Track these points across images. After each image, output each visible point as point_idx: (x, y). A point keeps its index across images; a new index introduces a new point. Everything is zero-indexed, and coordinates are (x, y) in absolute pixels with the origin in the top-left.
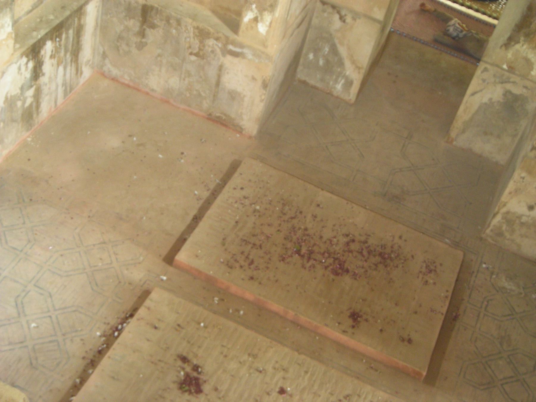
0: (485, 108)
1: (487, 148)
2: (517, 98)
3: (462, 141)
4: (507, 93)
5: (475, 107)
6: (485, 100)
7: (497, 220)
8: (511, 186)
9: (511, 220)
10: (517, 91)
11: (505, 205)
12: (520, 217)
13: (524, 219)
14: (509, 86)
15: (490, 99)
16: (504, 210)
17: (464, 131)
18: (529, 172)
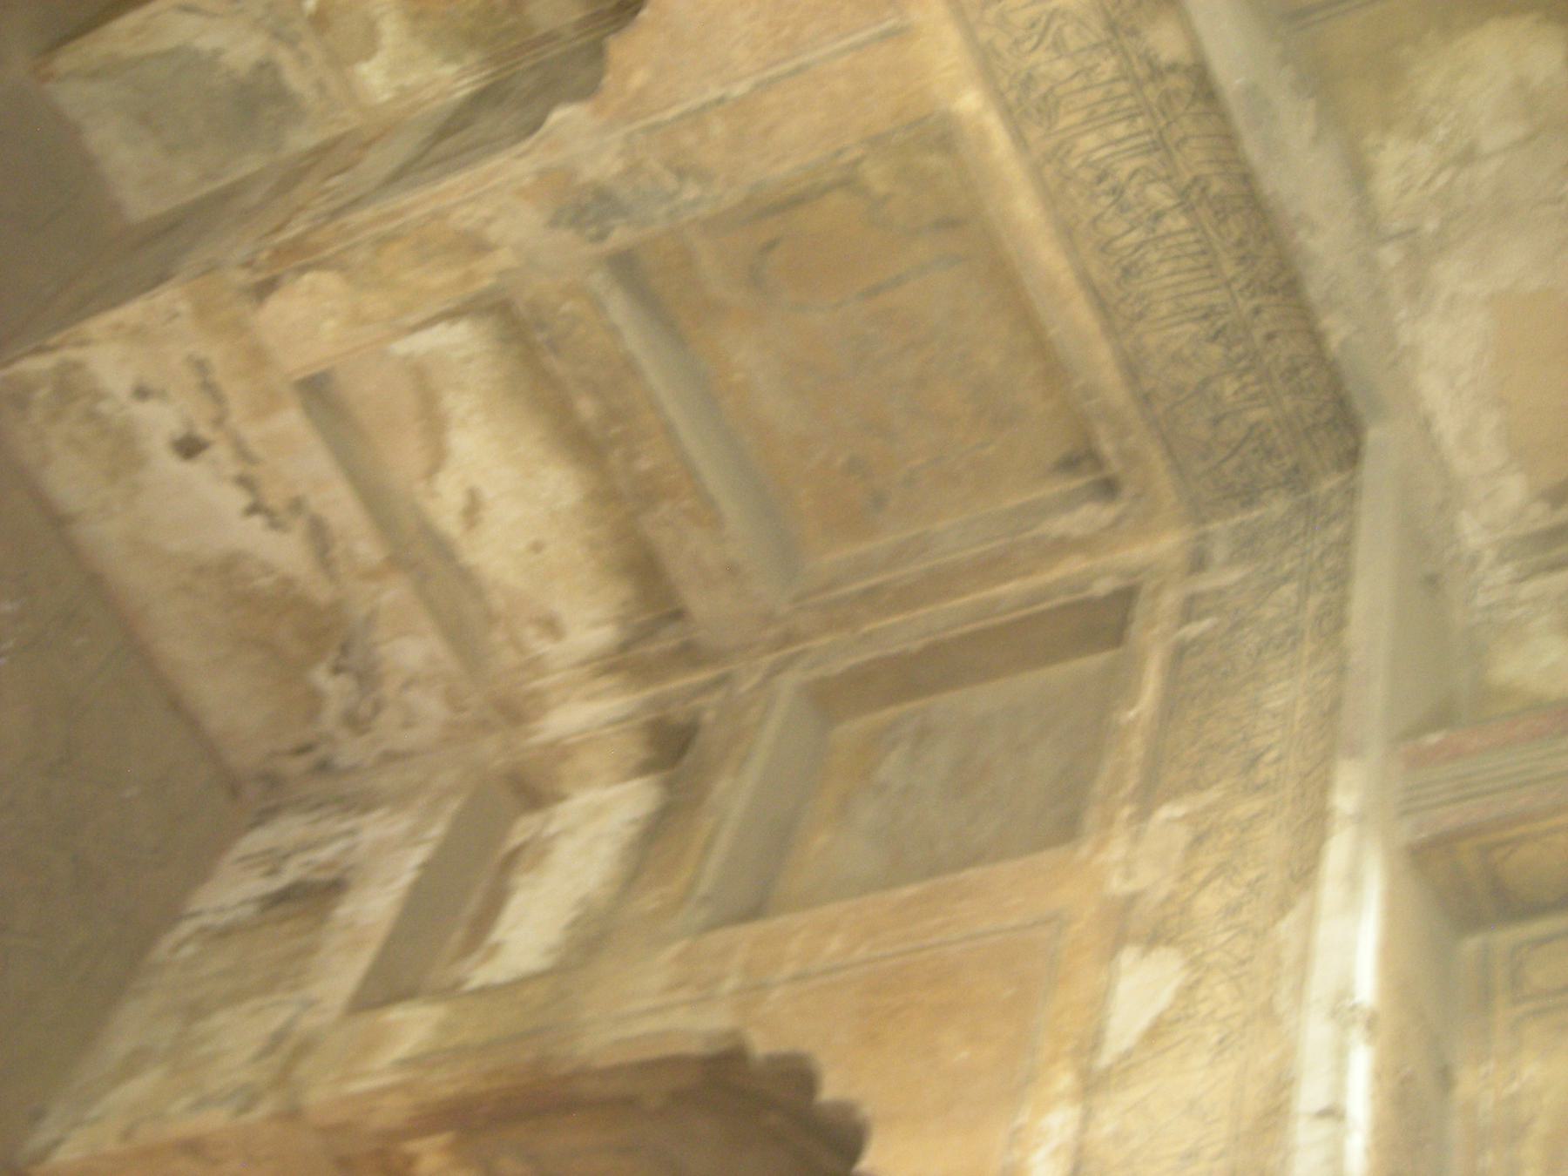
0: (189, 61)
1: (139, 174)
2: (281, 95)
3: (71, 96)
4: (266, 67)
5: (168, 43)
6: (206, 43)
7: (36, 365)
8: (132, 312)
9: (71, 387)
10: (296, 79)
11: (83, 343)
12: (100, 395)
13: (105, 407)
14: (284, 56)
15: (217, 53)
16: (72, 354)
17: (94, 75)
18: (202, 312)
